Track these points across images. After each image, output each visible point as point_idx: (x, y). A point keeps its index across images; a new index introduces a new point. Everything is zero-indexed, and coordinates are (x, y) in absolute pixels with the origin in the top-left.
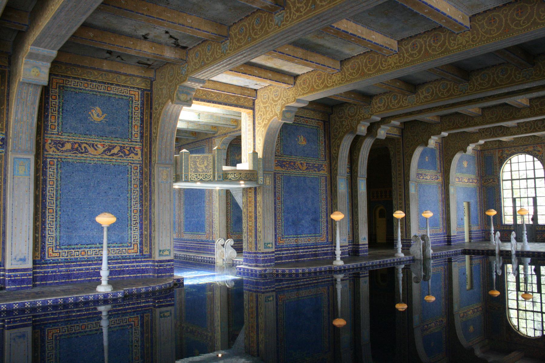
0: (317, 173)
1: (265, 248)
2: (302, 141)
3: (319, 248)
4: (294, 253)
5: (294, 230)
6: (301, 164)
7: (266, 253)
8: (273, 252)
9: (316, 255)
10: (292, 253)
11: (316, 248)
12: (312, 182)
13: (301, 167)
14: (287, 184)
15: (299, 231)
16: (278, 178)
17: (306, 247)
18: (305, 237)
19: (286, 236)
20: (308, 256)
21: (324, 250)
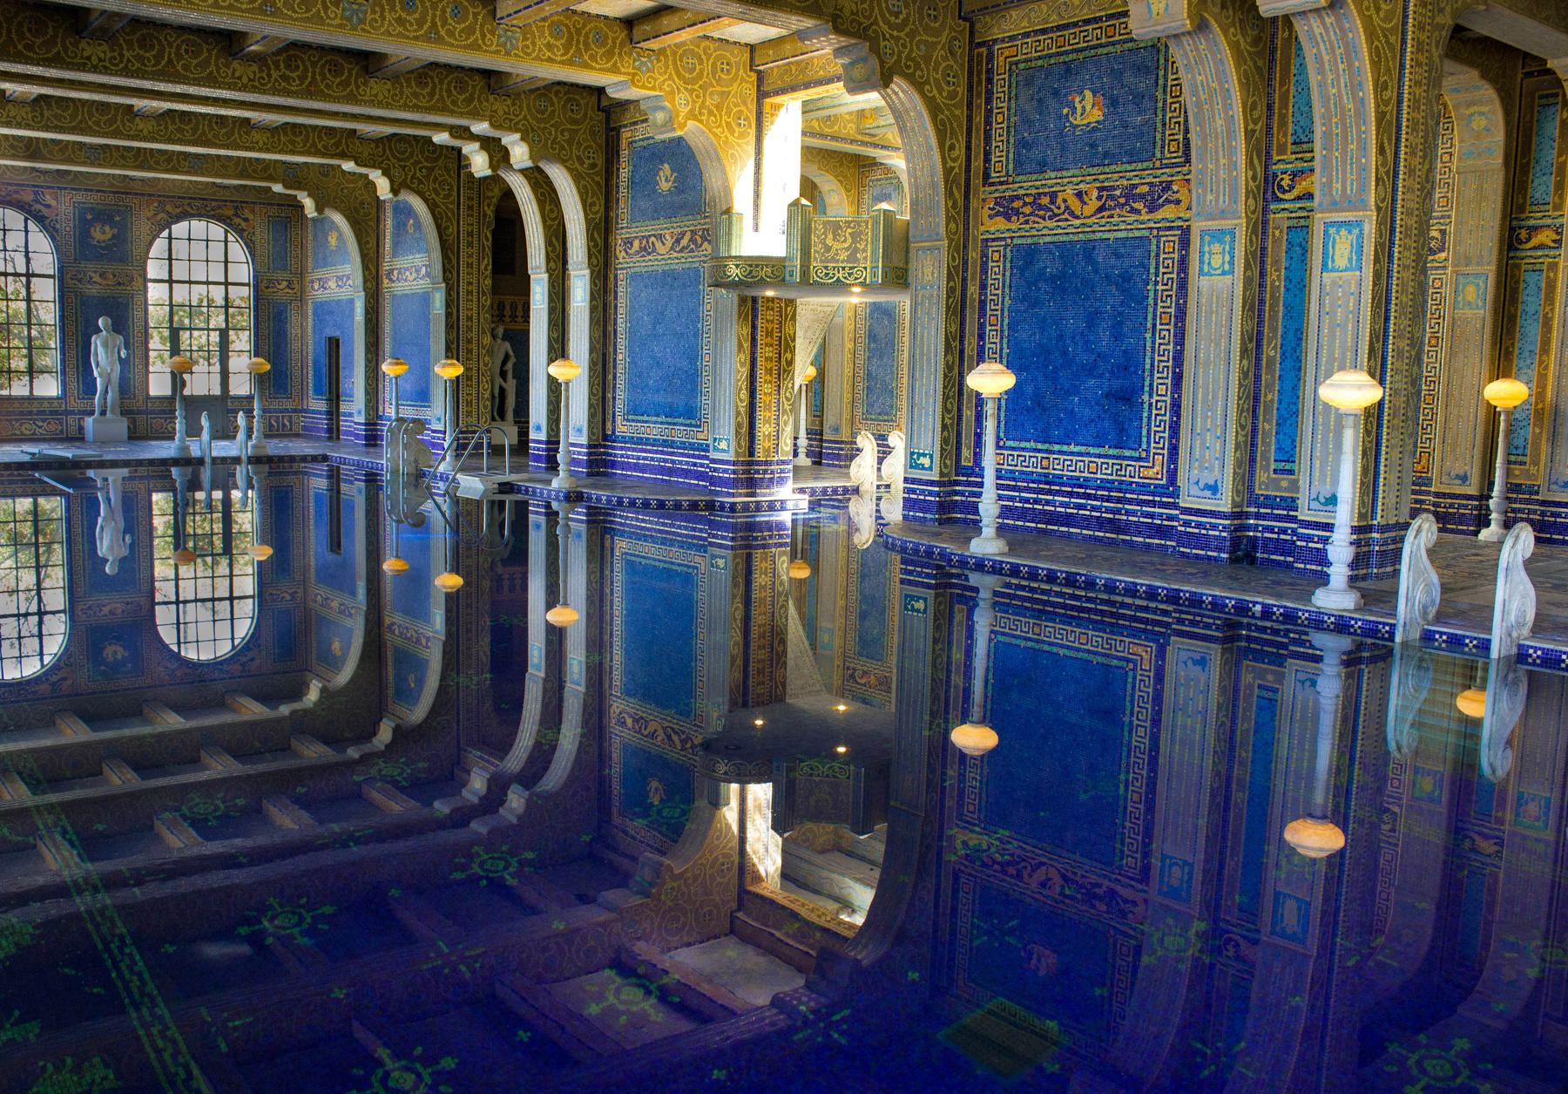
2: (1088, 110)
3: (1130, 501)
4: (1036, 501)
5: (1040, 426)
6: (1079, 195)
7: (913, 481)
8: (932, 483)
9: (1115, 526)
10: (1027, 501)
11: (1119, 500)
12: (1118, 256)
13: (1075, 204)
14: (1022, 270)
17: (1078, 486)
18: (1080, 454)
19: (1009, 443)
20: (1087, 522)
21: (1152, 516)
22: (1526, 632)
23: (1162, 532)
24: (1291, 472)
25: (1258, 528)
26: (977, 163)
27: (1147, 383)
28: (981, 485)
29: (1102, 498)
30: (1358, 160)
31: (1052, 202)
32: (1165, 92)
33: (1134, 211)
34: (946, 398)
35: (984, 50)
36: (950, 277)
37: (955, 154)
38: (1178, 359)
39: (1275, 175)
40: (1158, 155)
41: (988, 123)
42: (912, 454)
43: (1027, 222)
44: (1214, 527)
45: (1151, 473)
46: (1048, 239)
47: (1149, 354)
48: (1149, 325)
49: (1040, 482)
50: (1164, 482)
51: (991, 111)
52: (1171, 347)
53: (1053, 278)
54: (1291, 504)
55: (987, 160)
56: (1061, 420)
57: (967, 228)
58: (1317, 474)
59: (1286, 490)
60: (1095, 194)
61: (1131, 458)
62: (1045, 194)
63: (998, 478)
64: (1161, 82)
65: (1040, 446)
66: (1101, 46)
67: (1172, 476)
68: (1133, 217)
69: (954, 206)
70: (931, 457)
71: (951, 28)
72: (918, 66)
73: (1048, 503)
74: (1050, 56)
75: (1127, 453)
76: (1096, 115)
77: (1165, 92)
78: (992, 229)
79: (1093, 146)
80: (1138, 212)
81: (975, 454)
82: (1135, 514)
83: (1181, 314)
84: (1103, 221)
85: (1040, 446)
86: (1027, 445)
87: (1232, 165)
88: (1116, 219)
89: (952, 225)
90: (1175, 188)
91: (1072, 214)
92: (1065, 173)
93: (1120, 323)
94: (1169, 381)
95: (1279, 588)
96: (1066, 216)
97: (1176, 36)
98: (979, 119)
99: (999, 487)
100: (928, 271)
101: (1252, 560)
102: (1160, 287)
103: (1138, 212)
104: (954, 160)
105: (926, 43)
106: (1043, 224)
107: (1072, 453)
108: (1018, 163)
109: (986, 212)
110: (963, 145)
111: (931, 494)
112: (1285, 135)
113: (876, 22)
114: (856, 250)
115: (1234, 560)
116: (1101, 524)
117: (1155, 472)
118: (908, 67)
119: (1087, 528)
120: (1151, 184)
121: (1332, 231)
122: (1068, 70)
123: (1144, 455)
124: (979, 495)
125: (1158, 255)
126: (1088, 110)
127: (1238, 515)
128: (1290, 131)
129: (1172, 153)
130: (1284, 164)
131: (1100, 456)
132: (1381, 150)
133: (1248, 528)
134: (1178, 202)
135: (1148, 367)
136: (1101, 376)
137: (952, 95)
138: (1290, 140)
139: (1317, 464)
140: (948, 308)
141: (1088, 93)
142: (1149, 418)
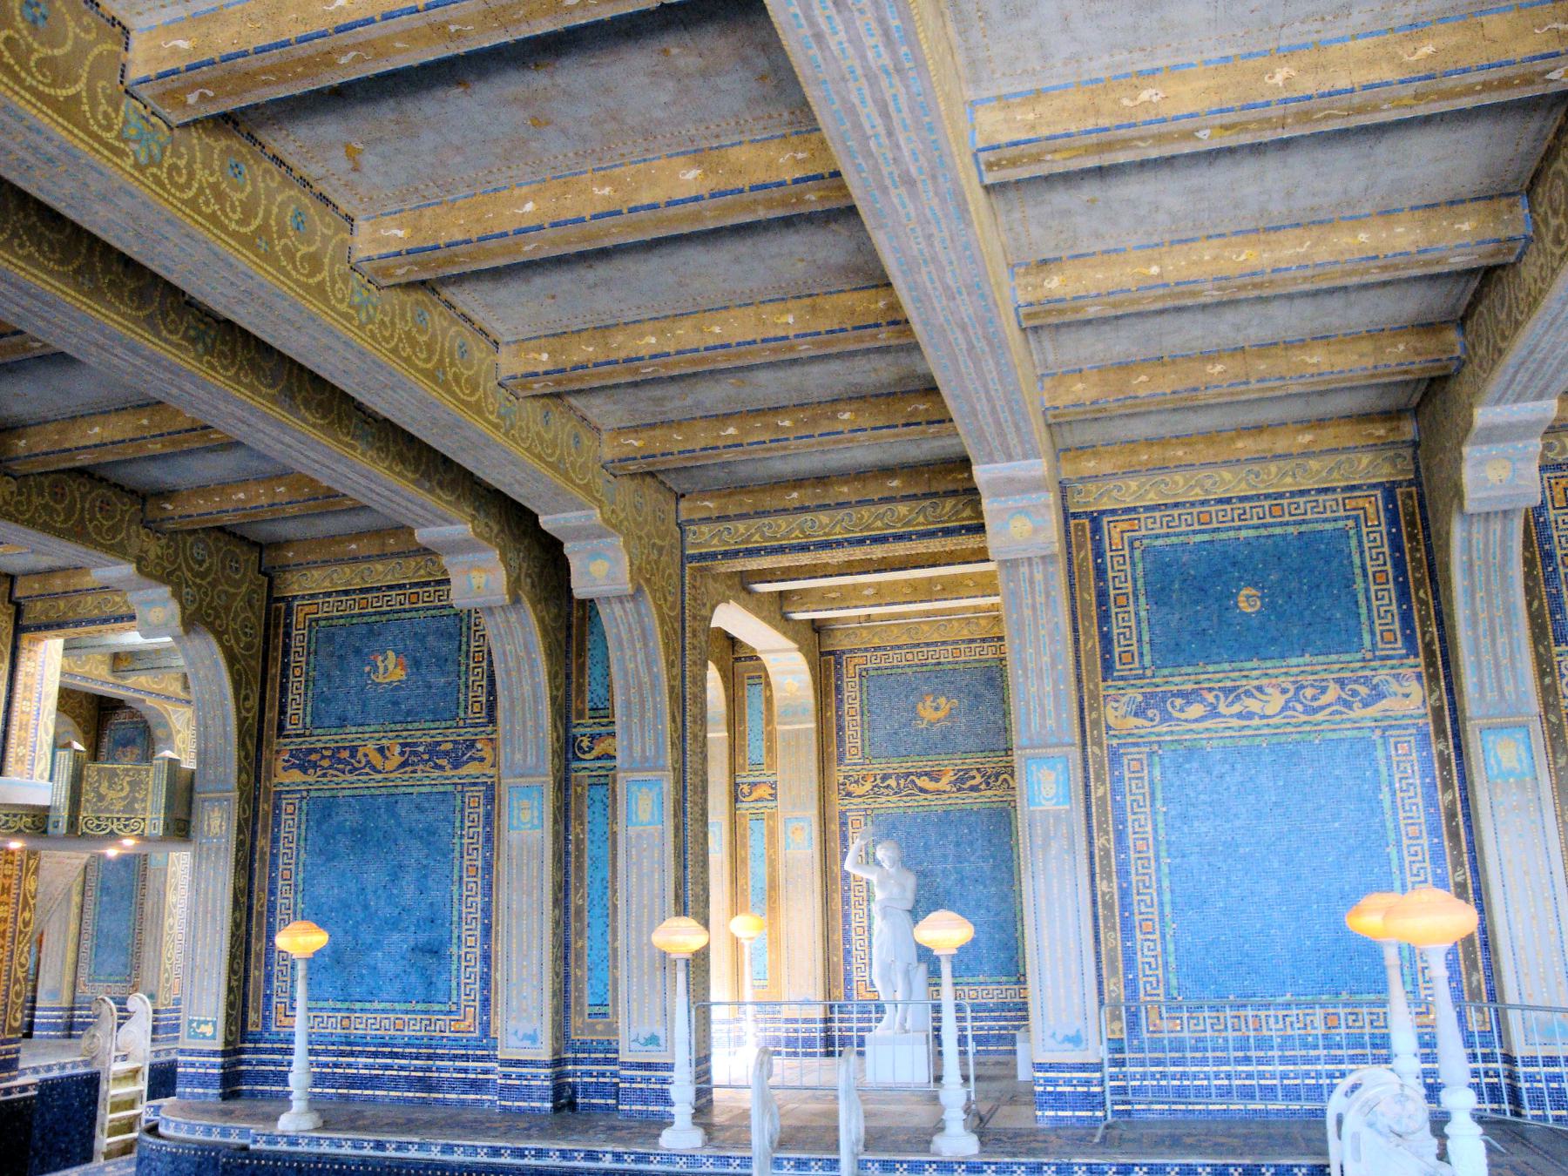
0: (449, 773)
1: (190, 1037)
2: (390, 669)
3: (441, 1057)
4: (336, 1065)
6: (381, 750)
8: (214, 1053)
9: (426, 1085)
10: (326, 1065)
11: (429, 1057)
13: (376, 759)
14: (319, 823)
15: (357, 991)
16: (290, 809)
17: (385, 1049)
18: (384, 1011)
20: (395, 1083)
21: (466, 1071)
22: (861, 1148)
23: (476, 1086)
24: (605, 1015)
25: (578, 1074)
26: (272, 715)
27: (455, 935)
28: (289, 1052)
29: (411, 1056)
30: (655, 725)
31: (353, 756)
32: (467, 656)
33: (437, 767)
34: (233, 957)
35: (282, 605)
36: (240, 830)
37: (248, 704)
38: (487, 911)
39: (575, 738)
40: (462, 715)
41: (284, 675)
42: (191, 1021)
43: (324, 775)
44: (535, 1077)
45: (462, 1026)
46: (347, 792)
47: (456, 906)
48: (456, 877)
49: (341, 1043)
50: (477, 1034)
51: (288, 664)
52: (478, 899)
53: (353, 831)
54: (611, 1048)
55: (283, 712)
56: (362, 976)
57: (258, 779)
58: (635, 1016)
59: (602, 1033)
60: (398, 749)
61: (441, 1012)
62: (345, 748)
63: (310, 1043)
64: (464, 647)
65: (339, 1005)
66: (405, 611)
67: (486, 1028)
68: (437, 773)
69: (246, 757)
70: (215, 1024)
71: (251, 582)
72: (217, 617)
73: (349, 1066)
74: (352, 616)
75: (437, 1007)
76: (399, 675)
77: (467, 656)
78: (287, 781)
79: (396, 703)
80: (442, 768)
81: (264, 1017)
82: (447, 1070)
83: (488, 867)
84: (406, 777)
85: (339, 1005)
86: (325, 1004)
87: (537, 727)
88: (419, 775)
89: (244, 777)
90: (479, 746)
91: (374, 768)
92: (367, 728)
93: (425, 876)
94: (478, 933)
95: (618, 1134)
96: (367, 770)
97: (490, 609)
98: (275, 671)
99: (311, 1052)
100: (216, 823)
101: (572, 1105)
102: (466, 841)
103: (442, 768)
104: (248, 711)
105: (226, 592)
106: (342, 777)
107: (376, 1011)
108: (316, 715)
109: (280, 764)
110: (257, 696)
111: (213, 1066)
112: (583, 702)
113: (179, 568)
114: (135, 800)
115: (557, 1109)
116: (411, 1083)
117: (468, 1024)
118: (209, 615)
119: (395, 1088)
120: (455, 742)
121: (634, 788)
122: (371, 631)
123: (454, 1008)
124: (290, 1064)
125: (462, 810)
126: (390, 669)
127: (558, 1062)
128: (588, 696)
129: (477, 712)
130: (583, 729)
131: (407, 1012)
132: (674, 720)
133: (568, 1075)
134: (482, 760)
135: (455, 919)
136: (406, 929)
137: (249, 647)
138: (588, 705)
139: (634, 1005)
140: (237, 861)
141: (391, 654)
142: (458, 970)
